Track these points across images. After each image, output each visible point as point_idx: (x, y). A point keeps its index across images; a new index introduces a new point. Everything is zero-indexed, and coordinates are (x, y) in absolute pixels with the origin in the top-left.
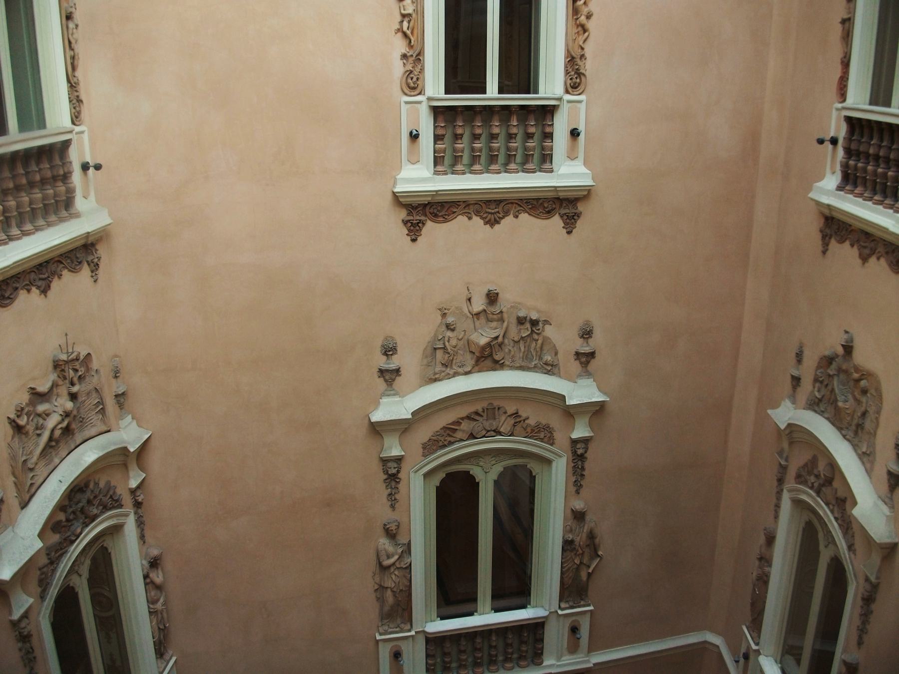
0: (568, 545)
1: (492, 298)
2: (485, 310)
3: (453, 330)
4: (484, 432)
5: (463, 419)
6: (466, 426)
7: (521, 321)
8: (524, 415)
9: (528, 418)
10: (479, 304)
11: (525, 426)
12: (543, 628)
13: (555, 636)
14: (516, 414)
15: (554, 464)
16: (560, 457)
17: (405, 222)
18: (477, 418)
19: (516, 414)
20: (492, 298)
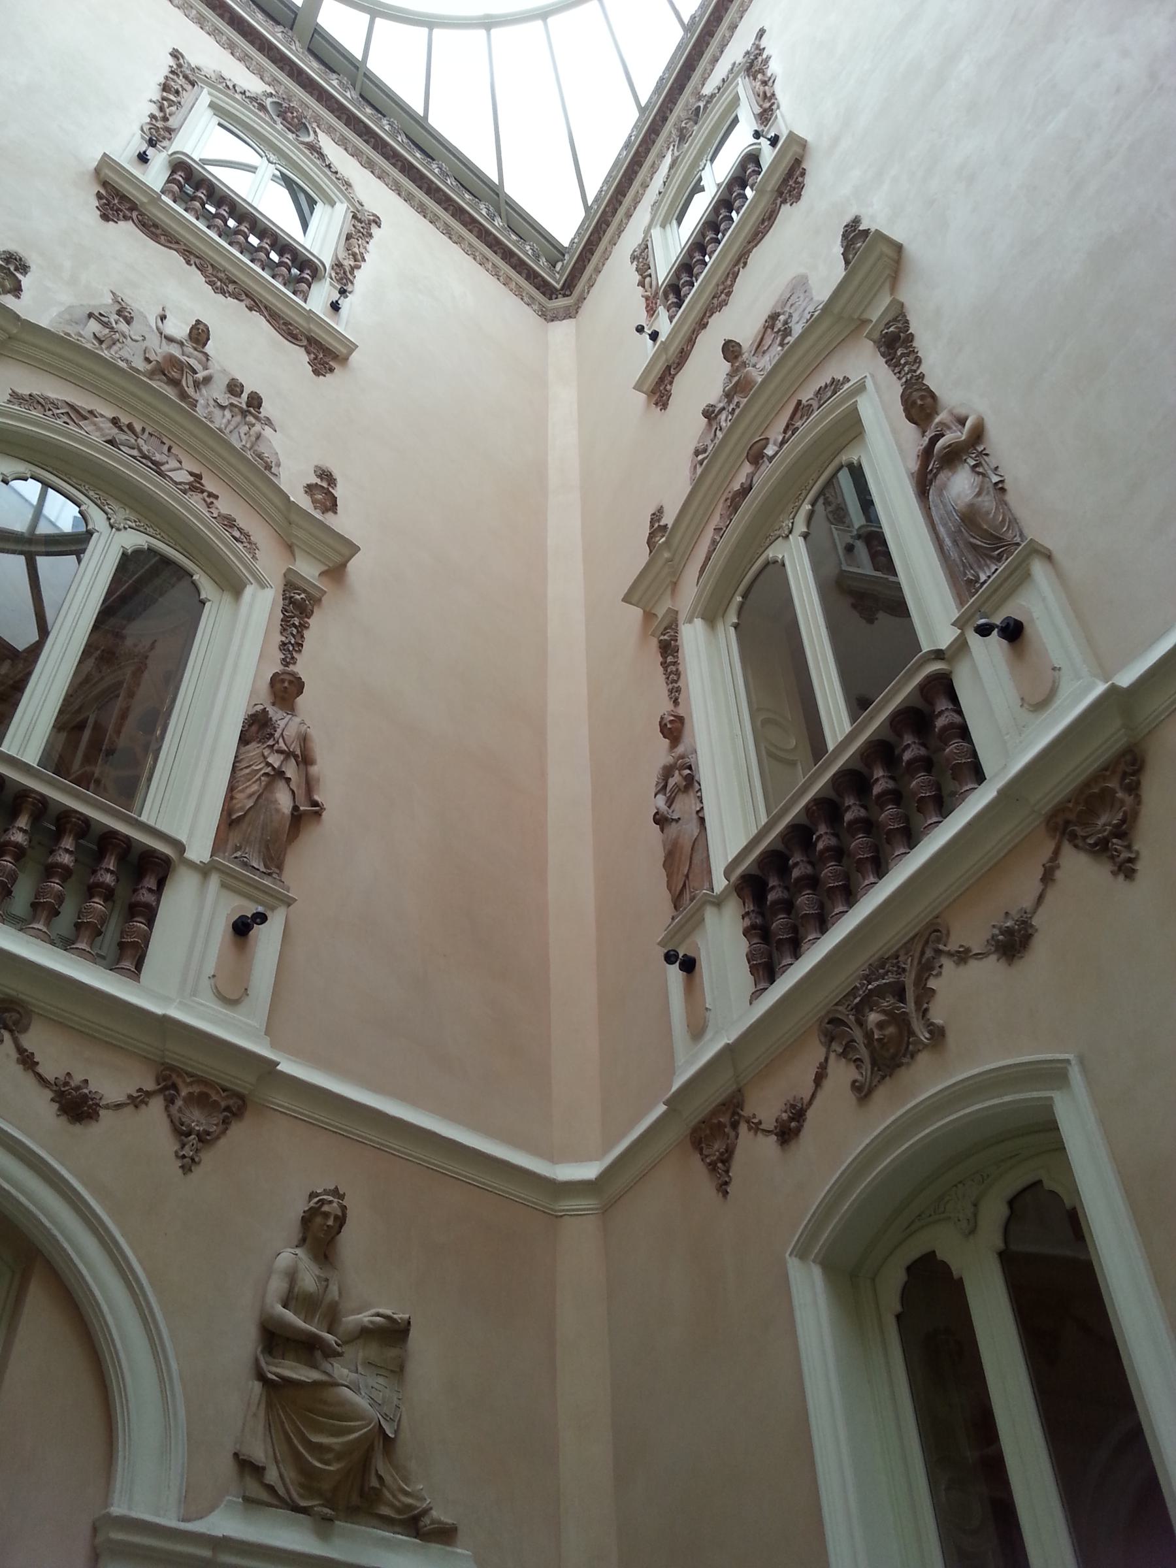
0: (257, 727)
1: (199, 335)
2: (181, 344)
3: (129, 321)
4: (135, 453)
5: (102, 416)
6: (108, 427)
7: (234, 388)
8: (210, 484)
9: (217, 497)
10: (178, 328)
11: (209, 500)
12: (161, 883)
13: (190, 916)
14: (198, 477)
15: (249, 591)
16: (262, 585)
17: (99, 196)
18: (125, 429)
19: (198, 477)
20: (199, 335)
